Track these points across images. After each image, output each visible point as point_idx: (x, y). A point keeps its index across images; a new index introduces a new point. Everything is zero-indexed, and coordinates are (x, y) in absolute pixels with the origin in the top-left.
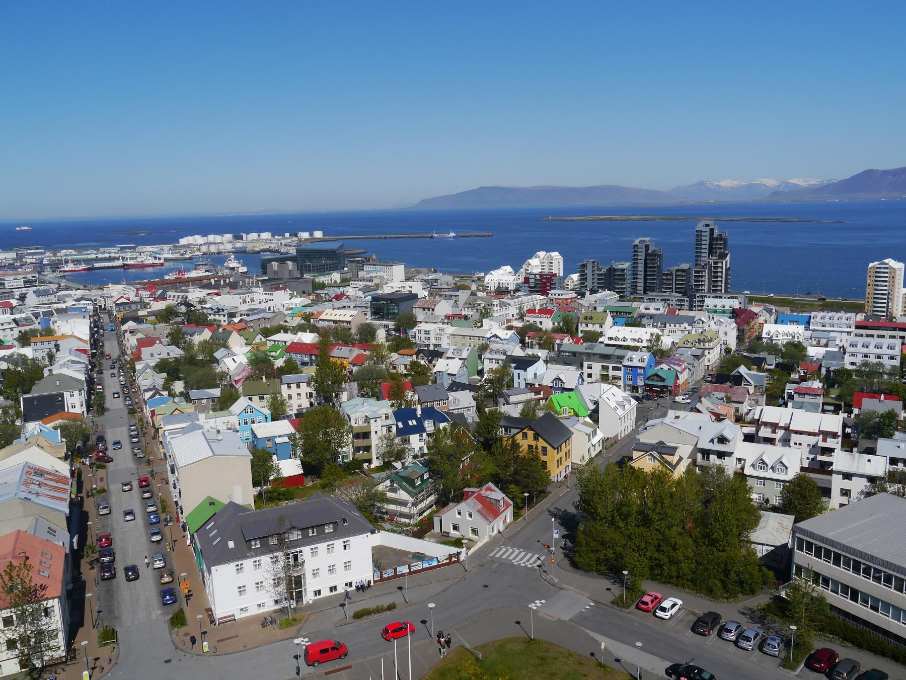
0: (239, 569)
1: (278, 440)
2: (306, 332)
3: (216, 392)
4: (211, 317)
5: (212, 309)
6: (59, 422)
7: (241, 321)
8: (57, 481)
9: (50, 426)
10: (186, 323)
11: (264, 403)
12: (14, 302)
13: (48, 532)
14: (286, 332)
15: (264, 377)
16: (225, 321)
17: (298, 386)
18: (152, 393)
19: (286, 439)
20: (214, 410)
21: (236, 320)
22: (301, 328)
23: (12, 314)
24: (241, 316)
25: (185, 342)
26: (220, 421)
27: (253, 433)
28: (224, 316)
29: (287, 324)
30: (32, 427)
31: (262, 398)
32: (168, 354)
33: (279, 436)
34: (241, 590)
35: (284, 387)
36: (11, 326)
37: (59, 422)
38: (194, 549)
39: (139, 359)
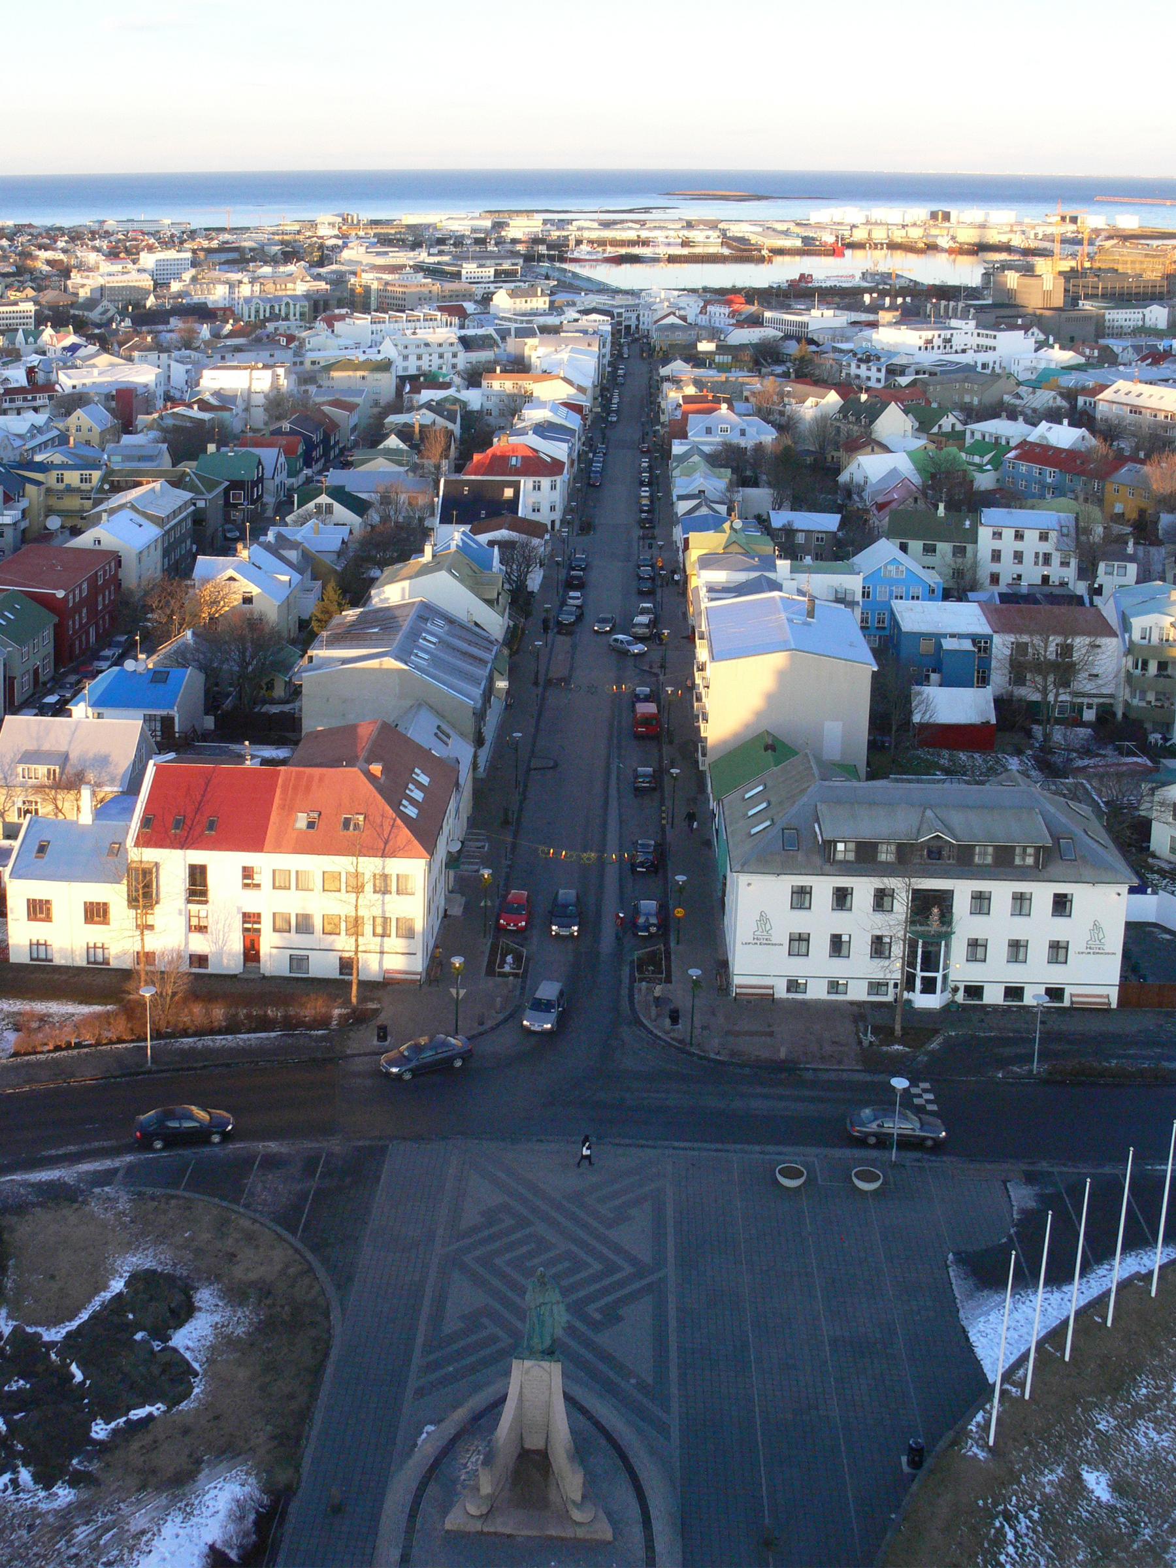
0: (801, 897)
1: (948, 644)
2: (1060, 423)
3: (829, 522)
4: (853, 370)
5: (855, 355)
6: (503, 534)
7: (913, 383)
8: (470, 643)
9: (483, 538)
10: (793, 376)
11: (929, 560)
12: (470, 307)
13: (436, 734)
14: (1012, 417)
15: (941, 506)
16: (879, 380)
17: (1019, 536)
18: (692, 503)
19: (967, 645)
20: (818, 557)
21: (904, 381)
22: (1054, 416)
23: (462, 327)
24: (917, 373)
25: (782, 413)
26: (822, 582)
27: (892, 613)
28: (879, 370)
29: (1018, 402)
30: (455, 535)
31: (929, 550)
32: (743, 433)
33: (953, 636)
34: (799, 943)
35: (984, 533)
36: (454, 349)
37: (503, 534)
38: (717, 830)
39: (684, 436)
